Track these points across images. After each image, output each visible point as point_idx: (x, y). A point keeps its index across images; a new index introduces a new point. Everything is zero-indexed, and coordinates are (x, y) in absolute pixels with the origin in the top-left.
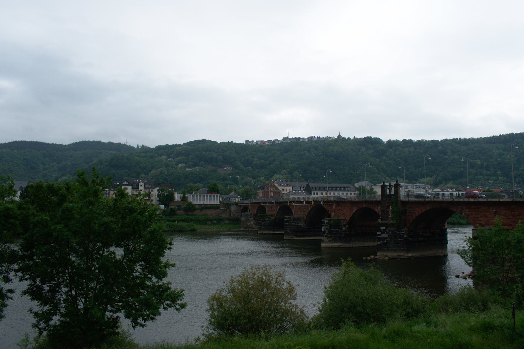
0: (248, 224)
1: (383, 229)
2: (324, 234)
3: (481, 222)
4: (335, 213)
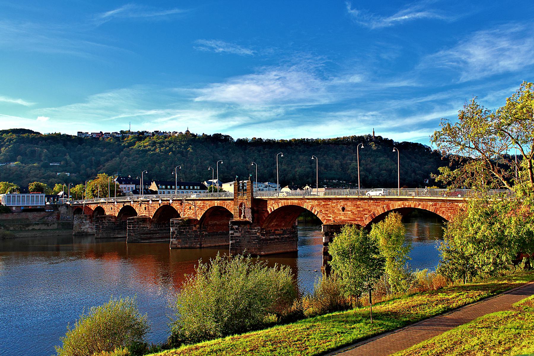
0: (82, 228)
1: (236, 228)
3: (330, 218)
4: (185, 213)
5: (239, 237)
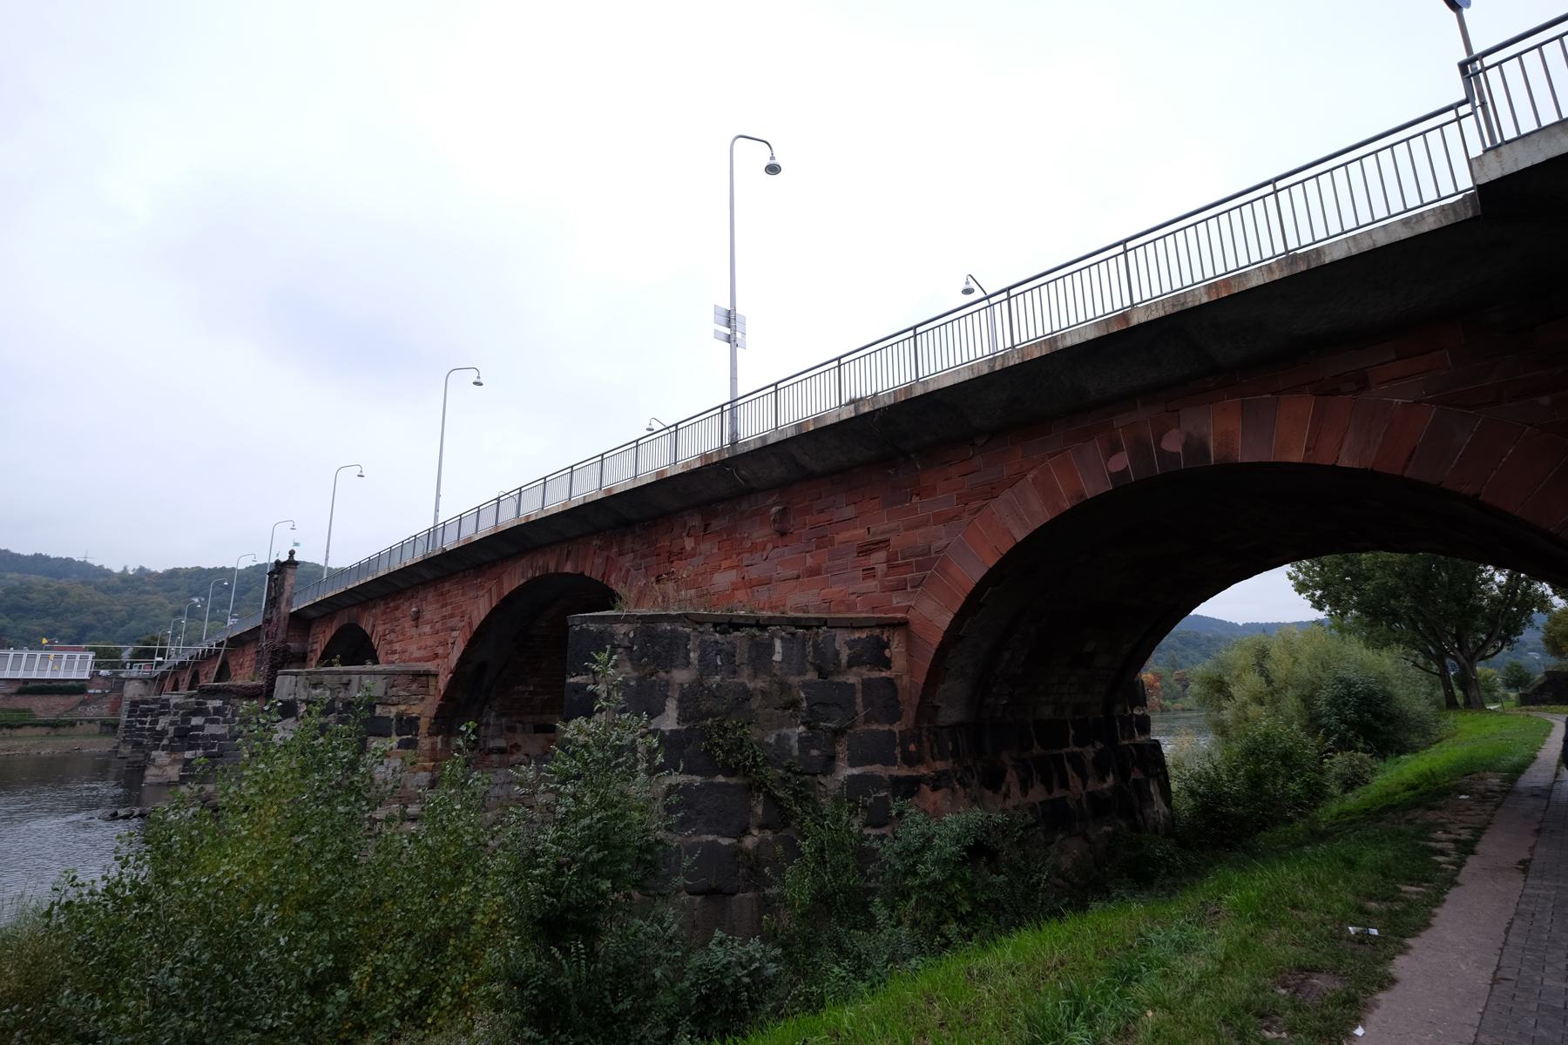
1: (214, 708)
2: (161, 740)
5: (222, 737)
